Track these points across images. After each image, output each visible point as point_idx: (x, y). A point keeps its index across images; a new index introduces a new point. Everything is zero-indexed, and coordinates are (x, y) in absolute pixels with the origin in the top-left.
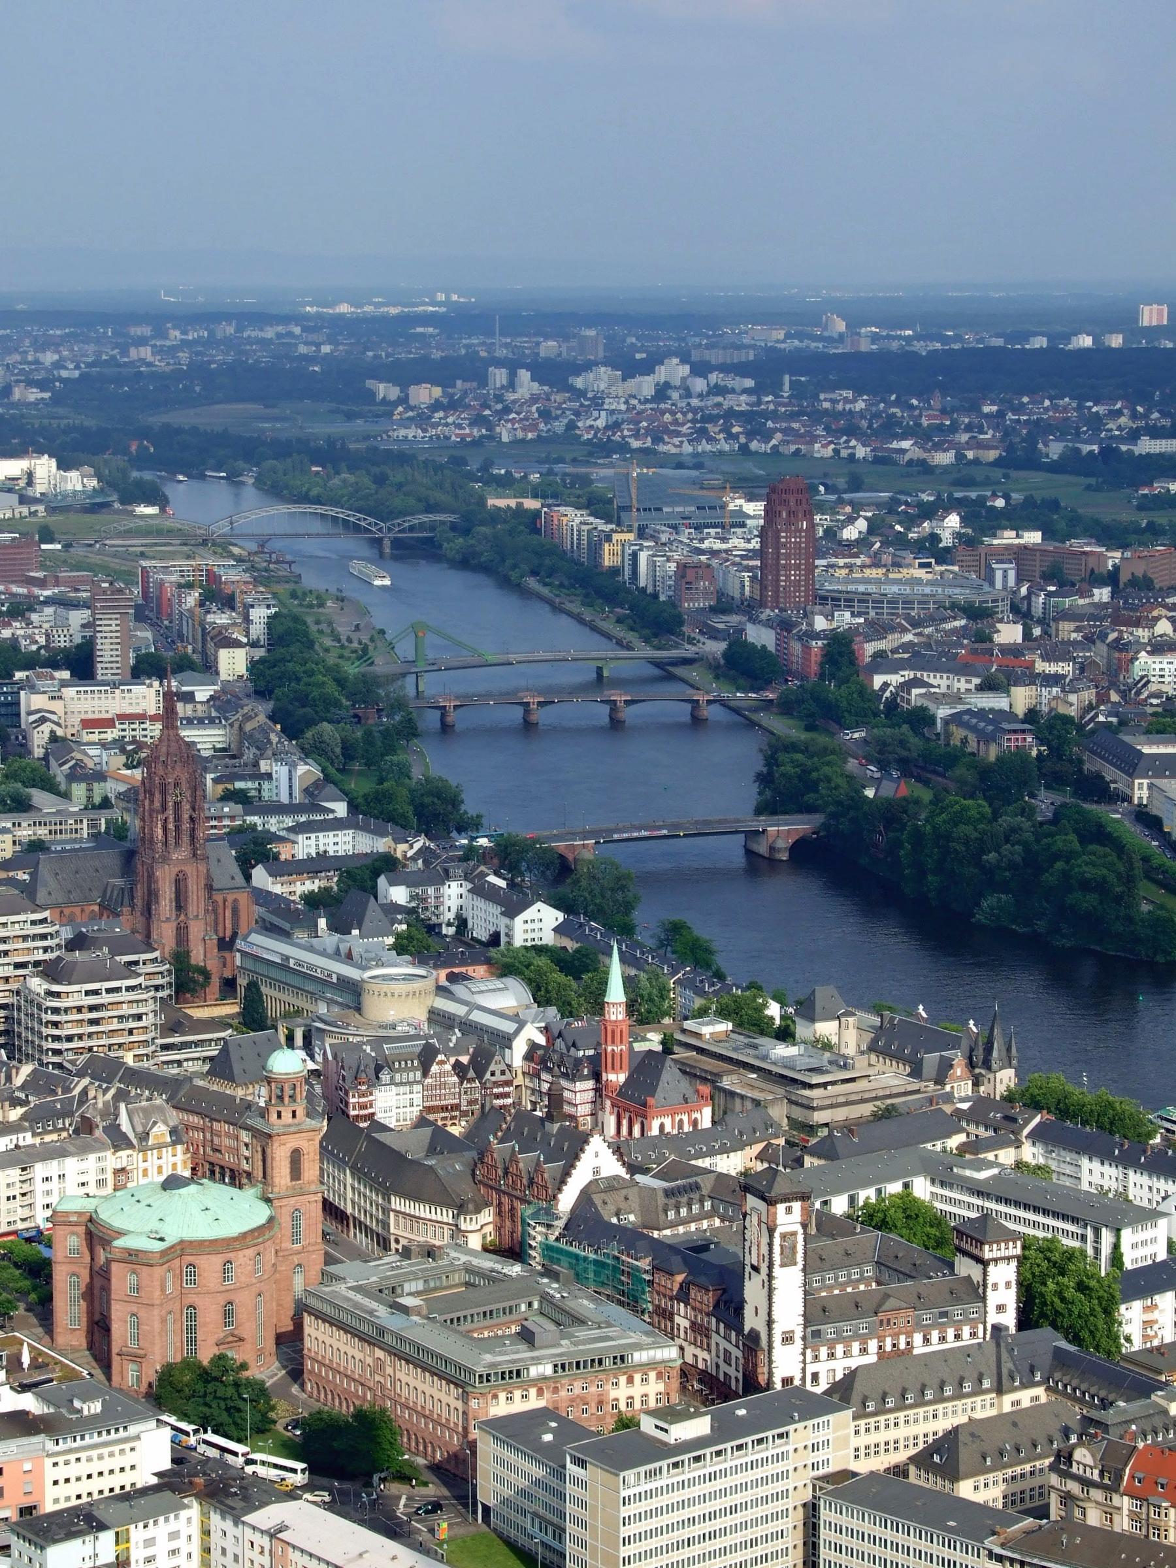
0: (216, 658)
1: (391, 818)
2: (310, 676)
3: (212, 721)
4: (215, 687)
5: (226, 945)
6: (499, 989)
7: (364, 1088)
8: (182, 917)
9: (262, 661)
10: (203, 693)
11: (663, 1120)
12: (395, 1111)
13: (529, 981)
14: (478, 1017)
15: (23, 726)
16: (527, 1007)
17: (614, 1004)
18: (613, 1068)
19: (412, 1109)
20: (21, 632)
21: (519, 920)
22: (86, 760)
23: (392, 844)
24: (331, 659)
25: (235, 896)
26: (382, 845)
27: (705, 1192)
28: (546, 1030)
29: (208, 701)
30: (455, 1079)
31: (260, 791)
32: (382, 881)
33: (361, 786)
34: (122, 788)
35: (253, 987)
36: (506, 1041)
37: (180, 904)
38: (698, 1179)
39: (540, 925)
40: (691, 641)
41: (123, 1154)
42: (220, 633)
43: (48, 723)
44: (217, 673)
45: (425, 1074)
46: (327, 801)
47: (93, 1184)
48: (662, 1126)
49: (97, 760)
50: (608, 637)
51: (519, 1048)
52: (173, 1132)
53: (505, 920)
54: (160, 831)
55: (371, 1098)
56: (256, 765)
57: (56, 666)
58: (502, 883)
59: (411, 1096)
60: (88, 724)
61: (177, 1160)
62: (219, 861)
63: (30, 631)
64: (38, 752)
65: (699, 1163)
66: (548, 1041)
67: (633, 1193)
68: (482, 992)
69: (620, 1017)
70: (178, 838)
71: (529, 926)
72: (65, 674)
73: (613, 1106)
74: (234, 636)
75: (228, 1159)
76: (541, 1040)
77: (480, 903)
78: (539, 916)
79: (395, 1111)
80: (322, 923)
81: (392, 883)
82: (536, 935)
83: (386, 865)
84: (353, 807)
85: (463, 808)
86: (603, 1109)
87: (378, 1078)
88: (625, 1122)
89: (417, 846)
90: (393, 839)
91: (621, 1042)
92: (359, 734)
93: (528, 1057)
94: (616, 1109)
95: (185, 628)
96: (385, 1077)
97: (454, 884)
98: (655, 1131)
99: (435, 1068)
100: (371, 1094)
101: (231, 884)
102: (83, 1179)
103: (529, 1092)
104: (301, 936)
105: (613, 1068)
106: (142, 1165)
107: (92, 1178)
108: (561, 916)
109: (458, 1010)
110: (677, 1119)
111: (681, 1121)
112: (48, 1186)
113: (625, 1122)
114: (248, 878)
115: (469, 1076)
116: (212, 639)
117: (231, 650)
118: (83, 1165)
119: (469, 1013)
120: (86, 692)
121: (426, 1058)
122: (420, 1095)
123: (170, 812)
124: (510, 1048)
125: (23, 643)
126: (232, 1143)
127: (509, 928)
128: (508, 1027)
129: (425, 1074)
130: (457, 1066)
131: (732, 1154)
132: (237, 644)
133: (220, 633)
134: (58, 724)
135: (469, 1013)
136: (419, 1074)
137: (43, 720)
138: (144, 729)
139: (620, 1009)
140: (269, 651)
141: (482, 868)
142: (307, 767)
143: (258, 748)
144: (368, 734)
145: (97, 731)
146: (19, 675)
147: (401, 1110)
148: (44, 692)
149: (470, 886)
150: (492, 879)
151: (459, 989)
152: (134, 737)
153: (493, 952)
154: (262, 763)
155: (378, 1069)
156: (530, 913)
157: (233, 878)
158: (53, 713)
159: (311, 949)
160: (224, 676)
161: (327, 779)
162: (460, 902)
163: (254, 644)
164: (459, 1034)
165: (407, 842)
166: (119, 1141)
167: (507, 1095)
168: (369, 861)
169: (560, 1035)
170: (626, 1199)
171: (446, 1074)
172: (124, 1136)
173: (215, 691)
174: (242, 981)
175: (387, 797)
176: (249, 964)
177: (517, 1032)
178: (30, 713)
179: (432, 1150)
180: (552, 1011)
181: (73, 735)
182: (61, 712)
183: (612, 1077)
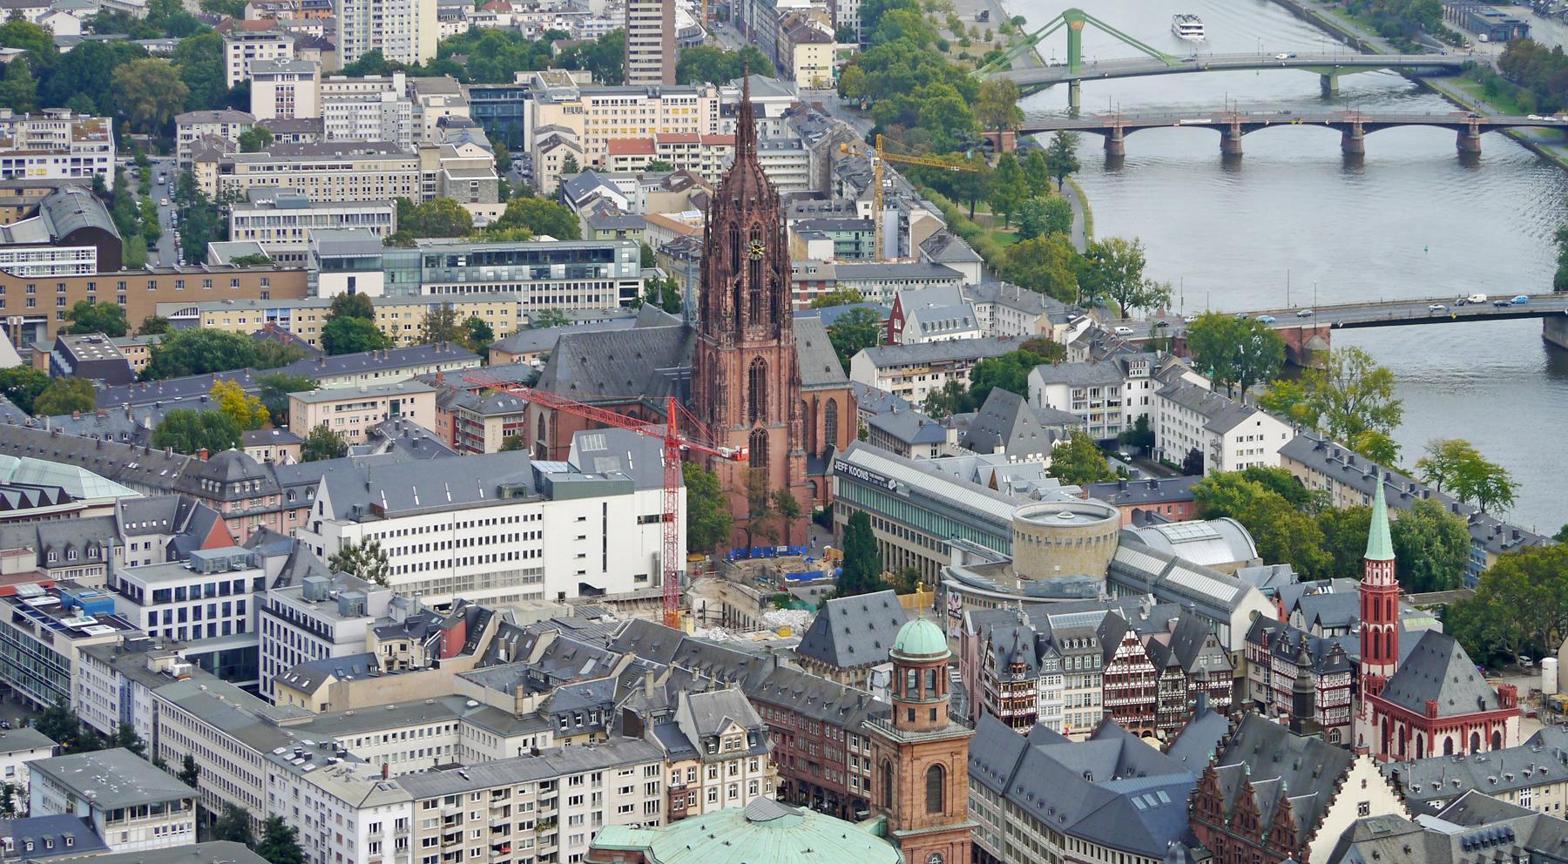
0: (791, 57)
1: (1045, 286)
2: (923, 85)
3: (789, 145)
4: (793, 98)
5: (819, 461)
6: (1209, 539)
7: (1021, 677)
8: (758, 425)
9: (854, 61)
10: (774, 107)
11: (1449, 734)
12: (1064, 712)
13: (1247, 526)
14: (1178, 576)
15: (527, 148)
16: (1247, 564)
17: (1378, 563)
18: (1376, 656)
19: (1088, 710)
20: (524, 18)
21: (1229, 438)
22: (616, 198)
23: (1048, 326)
24: (951, 60)
25: (830, 395)
26: (1032, 327)
27: (1520, 842)
28: (1275, 596)
29: (783, 117)
30: (1149, 667)
31: (857, 245)
32: (1035, 377)
33: (1001, 238)
34: (667, 239)
35: (860, 522)
36: (1222, 612)
37: (757, 407)
38: (1509, 823)
39: (1261, 444)
40: (1457, 41)
41: (683, 766)
42: (796, 22)
43: (562, 146)
44: (791, 78)
45: (1108, 658)
46: (953, 262)
47: (639, 808)
48: (1449, 744)
49: (631, 197)
50: (1337, 35)
51: (1241, 621)
52: (753, 734)
53: (1210, 436)
54: (729, 301)
55: (1030, 692)
56: (852, 207)
57: (570, 64)
58: (1204, 383)
59: (1087, 691)
60: (620, 147)
61: (760, 775)
62: (808, 344)
63: (535, 17)
64: (549, 186)
65: (1506, 799)
66: (1280, 614)
67: (1416, 842)
68: (1185, 541)
69: (1387, 582)
70: (754, 311)
71: (1246, 445)
72: (586, 77)
73: (1376, 711)
74: (817, 26)
75: (829, 777)
76: (1271, 612)
77: (1172, 411)
78: (1258, 431)
79: (1064, 712)
80: (953, 436)
81: (1049, 382)
82: (1255, 460)
83: (1043, 352)
84: (991, 270)
85: (1145, 274)
86: (1362, 715)
87: (1040, 663)
88: (1396, 736)
89: (1083, 327)
90: (1049, 317)
91: (1389, 618)
92: (993, 165)
93: (1251, 637)
94: (1381, 717)
95: (747, 15)
96: (1050, 661)
97: (1136, 385)
98: (1439, 750)
99: (1122, 651)
100: (1031, 686)
101: (825, 377)
102: (627, 800)
103: (1254, 687)
104: (920, 452)
105: (1376, 656)
106: (708, 782)
107: (638, 798)
108: (1290, 433)
109: (1154, 567)
110: (1470, 733)
111: (1476, 735)
112: (575, 810)
113: (1396, 736)
114: (847, 369)
115: (1170, 663)
116: (785, 30)
117: (812, 46)
118: (627, 781)
119: (1167, 570)
120: (614, 102)
121: (1110, 635)
122: (1100, 689)
123: (745, 273)
124: (1229, 624)
125: (526, 33)
126: (838, 755)
127: (1218, 447)
128: (1224, 593)
129: (1108, 658)
130: (1153, 647)
131: (1553, 788)
132: (820, 38)
133: (796, 22)
134: (577, 148)
135: (1167, 570)
136: (1098, 659)
137: (555, 141)
138: (696, 156)
139: (1387, 570)
140: (863, 47)
141: (1176, 361)
142: (924, 213)
143: (856, 185)
144: (1007, 163)
145: (629, 157)
146: (522, 78)
147: (1073, 711)
148: (559, 102)
149: (1158, 386)
150: (1191, 377)
151: (1148, 535)
152: (681, 166)
153: (1194, 484)
154: (860, 205)
155: (1039, 651)
156: (1246, 427)
157: (828, 370)
158: (570, 131)
159: (938, 472)
160: (802, 79)
161: (952, 227)
162: (1142, 410)
163: (843, 35)
164: (1153, 601)
165: (1068, 321)
166: (679, 745)
167: (1221, 693)
168: (1014, 348)
169: (1297, 606)
170: (1407, 850)
171: (1137, 660)
172: (684, 738)
173: (793, 104)
174: (841, 519)
175: (1039, 255)
176: (851, 493)
177: (1238, 599)
178: (537, 132)
179: (1122, 768)
180: (1286, 572)
181: (595, 162)
182: (580, 131)
183: (1376, 669)
